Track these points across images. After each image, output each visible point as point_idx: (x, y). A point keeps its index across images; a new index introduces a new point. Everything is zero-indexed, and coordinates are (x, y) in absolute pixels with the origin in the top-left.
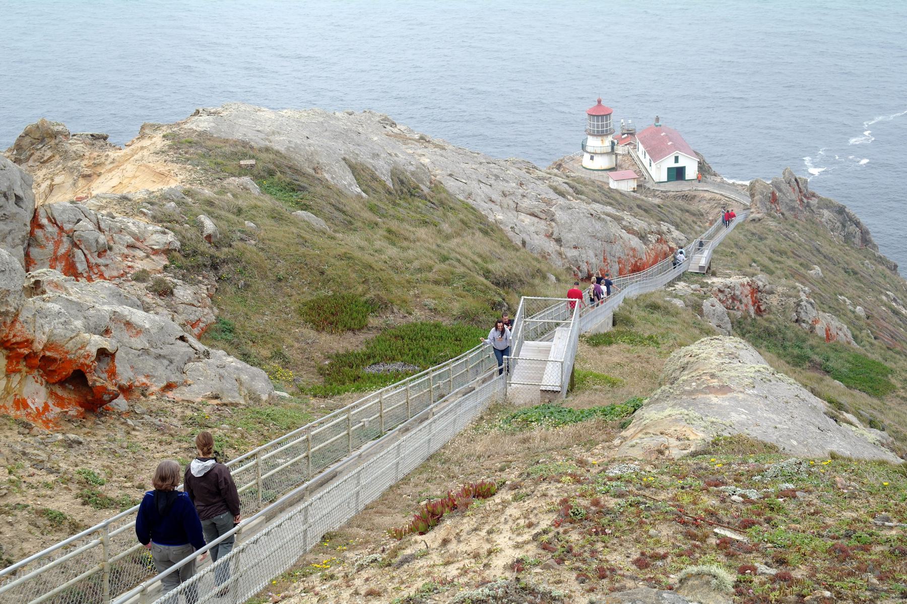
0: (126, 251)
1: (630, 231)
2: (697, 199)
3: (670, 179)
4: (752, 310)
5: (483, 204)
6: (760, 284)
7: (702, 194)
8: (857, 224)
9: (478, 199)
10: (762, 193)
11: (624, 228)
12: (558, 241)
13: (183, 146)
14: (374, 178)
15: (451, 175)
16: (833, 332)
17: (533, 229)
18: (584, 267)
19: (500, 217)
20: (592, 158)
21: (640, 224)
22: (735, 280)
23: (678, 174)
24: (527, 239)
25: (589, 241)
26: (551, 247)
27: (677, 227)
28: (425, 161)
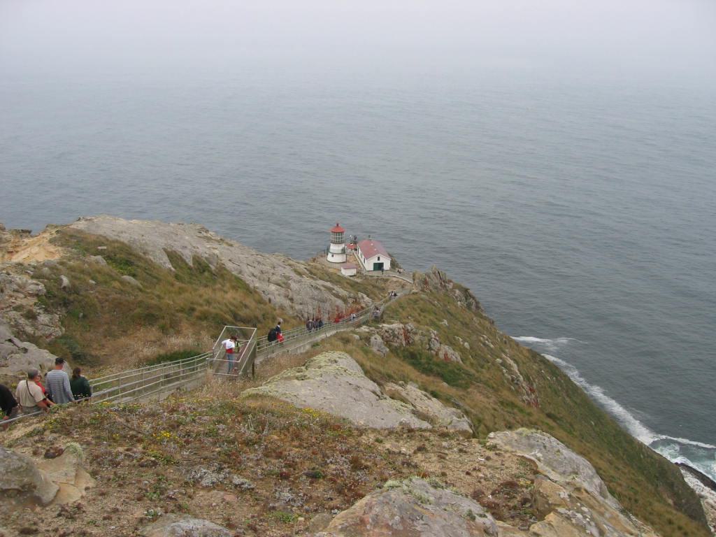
0: (12, 293)
1: (337, 296)
3: (375, 269)
4: (404, 343)
5: (248, 277)
6: (409, 328)
8: (474, 298)
9: (245, 275)
10: (419, 279)
11: (334, 294)
12: (291, 300)
13: (66, 238)
14: (183, 261)
15: (230, 260)
16: (449, 356)
17: (277, 292)
18: (306, 315)
19: (257, 285)
20: (333, 256)
21: (343, 292)
22: (396, 326)
23: (379, 267)
24: (272, 297)
25: (309, 301)
26: (287, 303)
27: (368, 296)
28: (216, 252)
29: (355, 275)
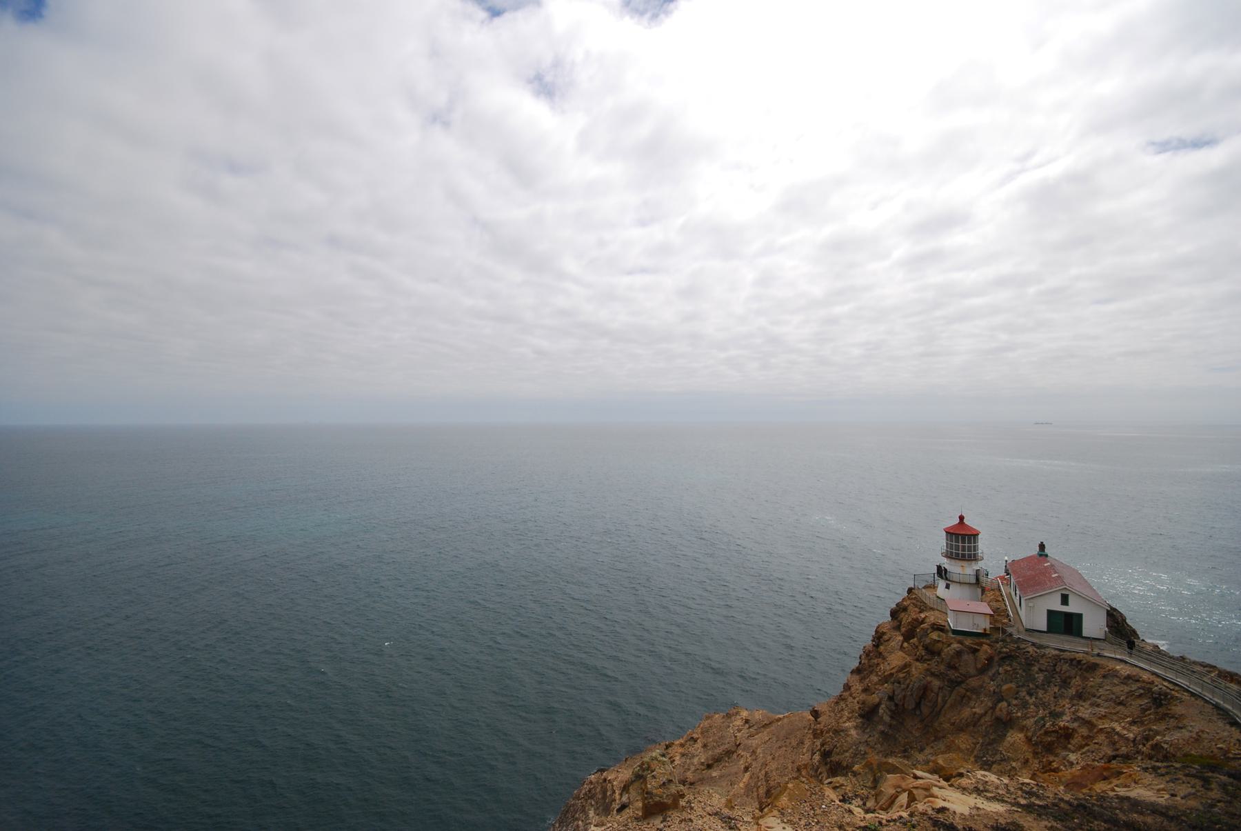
2: (1101, 672)
7: (1111, 665)
23: (1066, 624)
29: (984, 635)
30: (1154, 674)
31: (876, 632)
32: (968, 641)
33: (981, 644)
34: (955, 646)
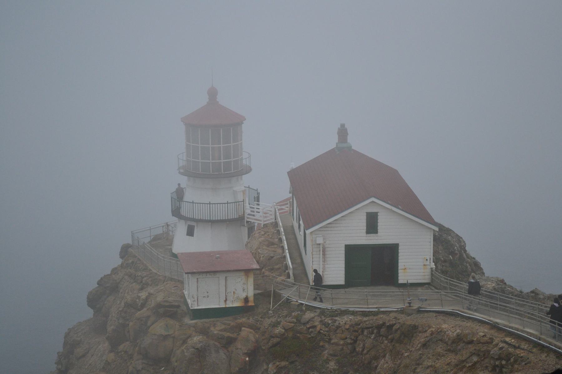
2: (421, 338)
3: (353, 278)
20: (190, 232)
23: (374, 265)
29: (245, 309)
30: (495, 327)
31: (65, 344)
32: (218, 327)
33: (239, 328)
34: (197, 339)
